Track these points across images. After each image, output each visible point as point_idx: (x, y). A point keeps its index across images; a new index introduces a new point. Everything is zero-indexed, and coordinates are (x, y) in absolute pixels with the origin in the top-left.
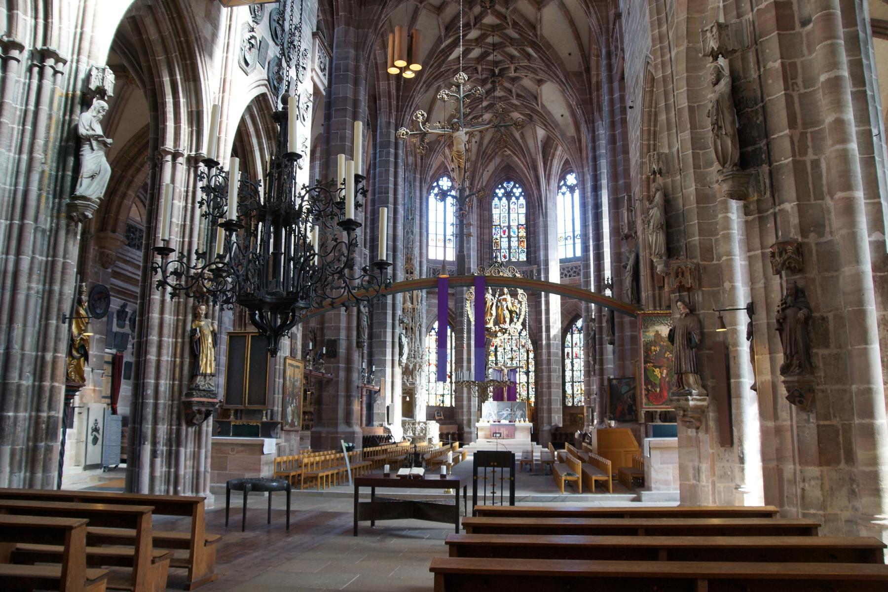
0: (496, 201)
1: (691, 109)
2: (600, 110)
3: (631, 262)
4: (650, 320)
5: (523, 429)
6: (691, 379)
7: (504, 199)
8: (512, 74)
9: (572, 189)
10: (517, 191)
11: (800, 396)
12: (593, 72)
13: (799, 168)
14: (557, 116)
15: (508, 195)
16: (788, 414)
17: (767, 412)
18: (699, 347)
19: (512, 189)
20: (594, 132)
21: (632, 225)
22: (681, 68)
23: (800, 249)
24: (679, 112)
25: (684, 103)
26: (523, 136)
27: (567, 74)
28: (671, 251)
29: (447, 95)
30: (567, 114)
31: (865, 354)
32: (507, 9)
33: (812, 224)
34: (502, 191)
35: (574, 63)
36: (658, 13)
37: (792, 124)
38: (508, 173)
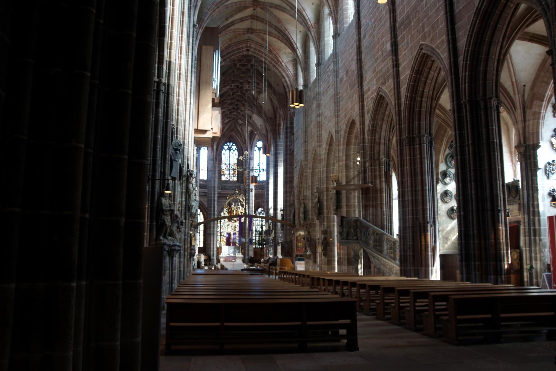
0: (223, 151)
1: (312, 186)
2: (279, 135)
3: (293, 212)
4: (298, 230)
5: (239, 258)
6: (308, 248)
7: (228, 151)
9: (259, 149)
10: (234, 147)
11: (325, 255)
12: (278, 119)
13: (327, 217)
14: (259, 125)
15: (229, 149)
16: (323, 257)
17: (321, 257)
18: (310, 241)
21: (294, 201)
22: (310, 175)
23: (326, 231)
24: (309, 186)
25: (310, 184)
26: (242, 129)
28: (305, 218)
31: (334, 249)
33: (329, 227)
34: (227, 147)
37: (327, 209)
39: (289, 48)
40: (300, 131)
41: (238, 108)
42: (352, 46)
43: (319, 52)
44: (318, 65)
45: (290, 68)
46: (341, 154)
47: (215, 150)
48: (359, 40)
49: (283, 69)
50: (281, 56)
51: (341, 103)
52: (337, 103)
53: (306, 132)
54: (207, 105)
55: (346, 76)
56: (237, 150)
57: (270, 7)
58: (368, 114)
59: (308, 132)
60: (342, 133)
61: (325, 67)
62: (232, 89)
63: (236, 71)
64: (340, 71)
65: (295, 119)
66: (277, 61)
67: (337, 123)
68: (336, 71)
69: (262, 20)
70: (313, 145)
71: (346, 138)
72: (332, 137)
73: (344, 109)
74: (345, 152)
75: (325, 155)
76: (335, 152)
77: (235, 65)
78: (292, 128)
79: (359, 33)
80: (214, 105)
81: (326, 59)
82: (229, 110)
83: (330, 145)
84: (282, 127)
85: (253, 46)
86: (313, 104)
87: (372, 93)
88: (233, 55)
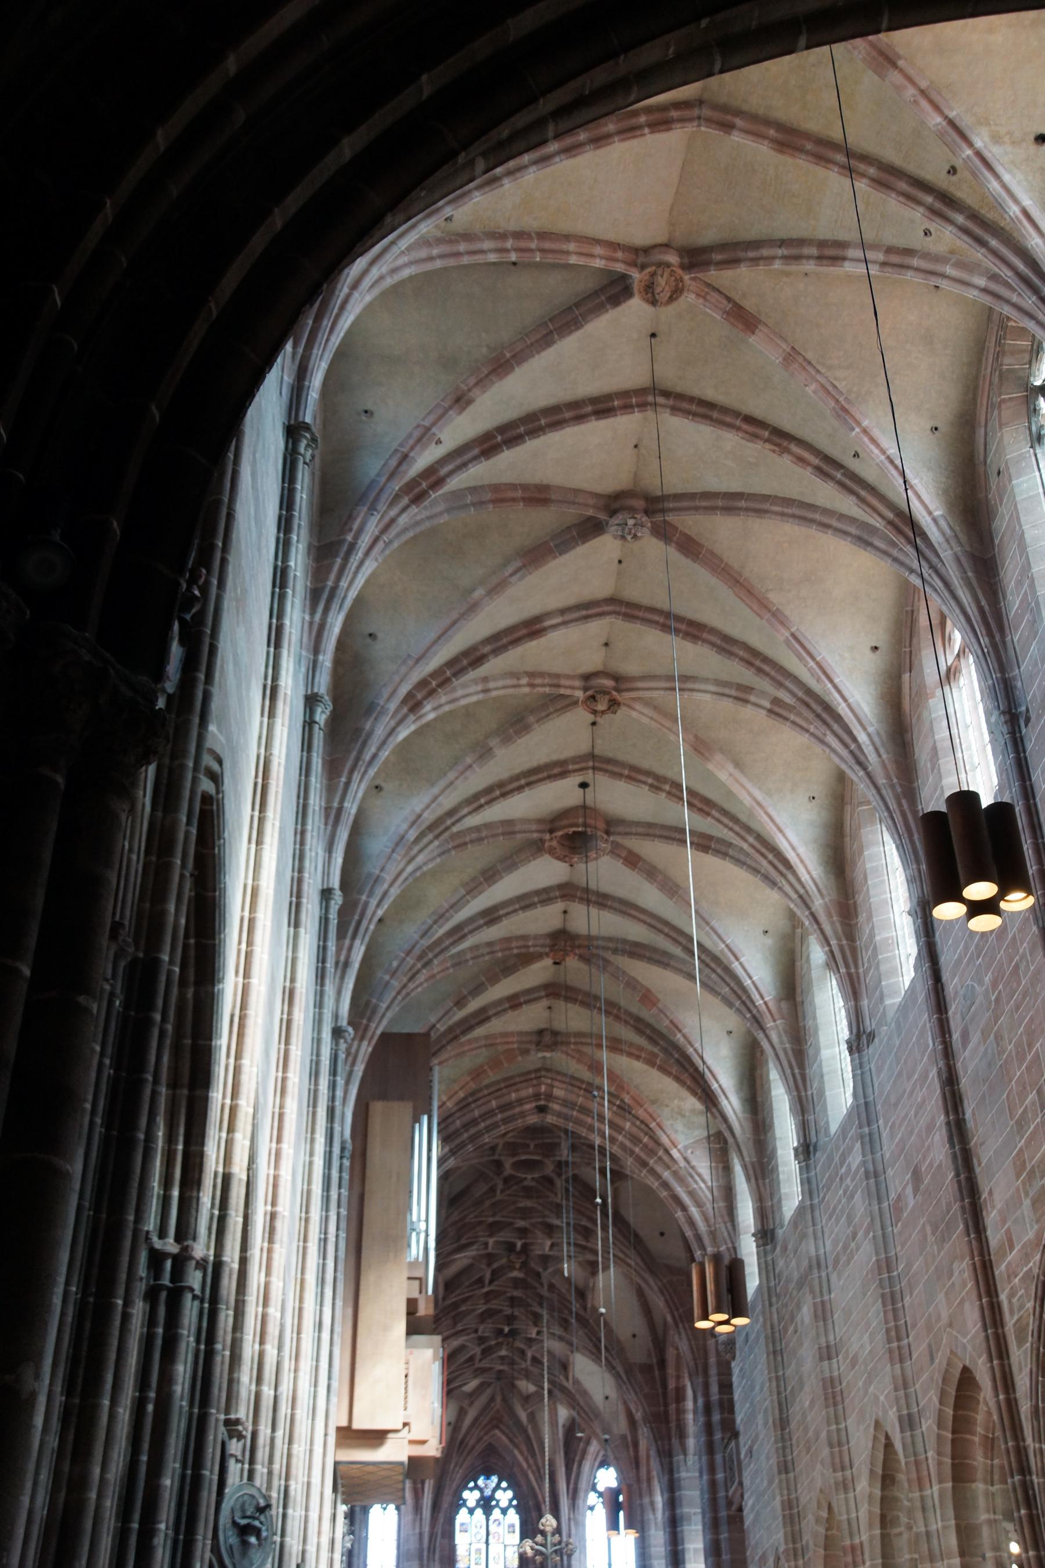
2: (682, 1435)
7: (479, 1512)
8: (534, 1335)
10: (504, 1497)
12: (671, 1371)
15: (487, 1504)
19: (494, 1490)
20: (671, 1472)
26: (532, 1417)
27: (629, 1369)
29: (532, 1548)
30: (613, 1394)
32: (545, 1269)
34: (476, 1494)
35: (640, 1352)
36: (794, 1542)
38: (489, 1462)
39: (694, 1093)
40: (760, 1420)
41: (513, 1333)
42: (924, 1076)
43: (805, 1105)
44: (806, 1150)
45: (703, 1165)
46: (936, 1525)
47: (427, 1512)
48: (948, 1053)
49: (675, 1174)
50: (667, 1124)
51: (907, 1300)
52: (892, 1300)
53: (783, 1423)
54: (386, 1328)
55: (916, 1190)
56: (517, 1508)
57: (615, 951)
58: (1021, 1342)
59: (793, 1425)
60: (928, 1425)
61: (830, 1158)
62: (490, 1258)
63: (500, 1187)
64: (890, 1172)
65: (736, 1367)
66: (654, 1147)
67: (903, 1384)
68: (876, 1175)
69: (588, 1000)
70: (819, 1483)
71: (948, 1449)
72: (889, 1445)
73: (921, 1323)
74: (950, 1512)
75: (871, 1526)
76: (910, 1512)
77: (498, 1164)
78: (728, 1407)
79: (943, 1028)
80: (415, 1327)
81: (834, 1127)
82: (482, 1340)
83: (887, 1479)
84: (689, 1404)
85: (558, 1092)
86: (799, 1307)
87: (1027, 1257)
88: (488, 1129)
